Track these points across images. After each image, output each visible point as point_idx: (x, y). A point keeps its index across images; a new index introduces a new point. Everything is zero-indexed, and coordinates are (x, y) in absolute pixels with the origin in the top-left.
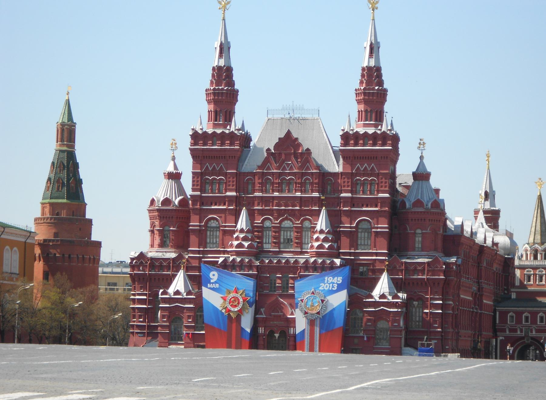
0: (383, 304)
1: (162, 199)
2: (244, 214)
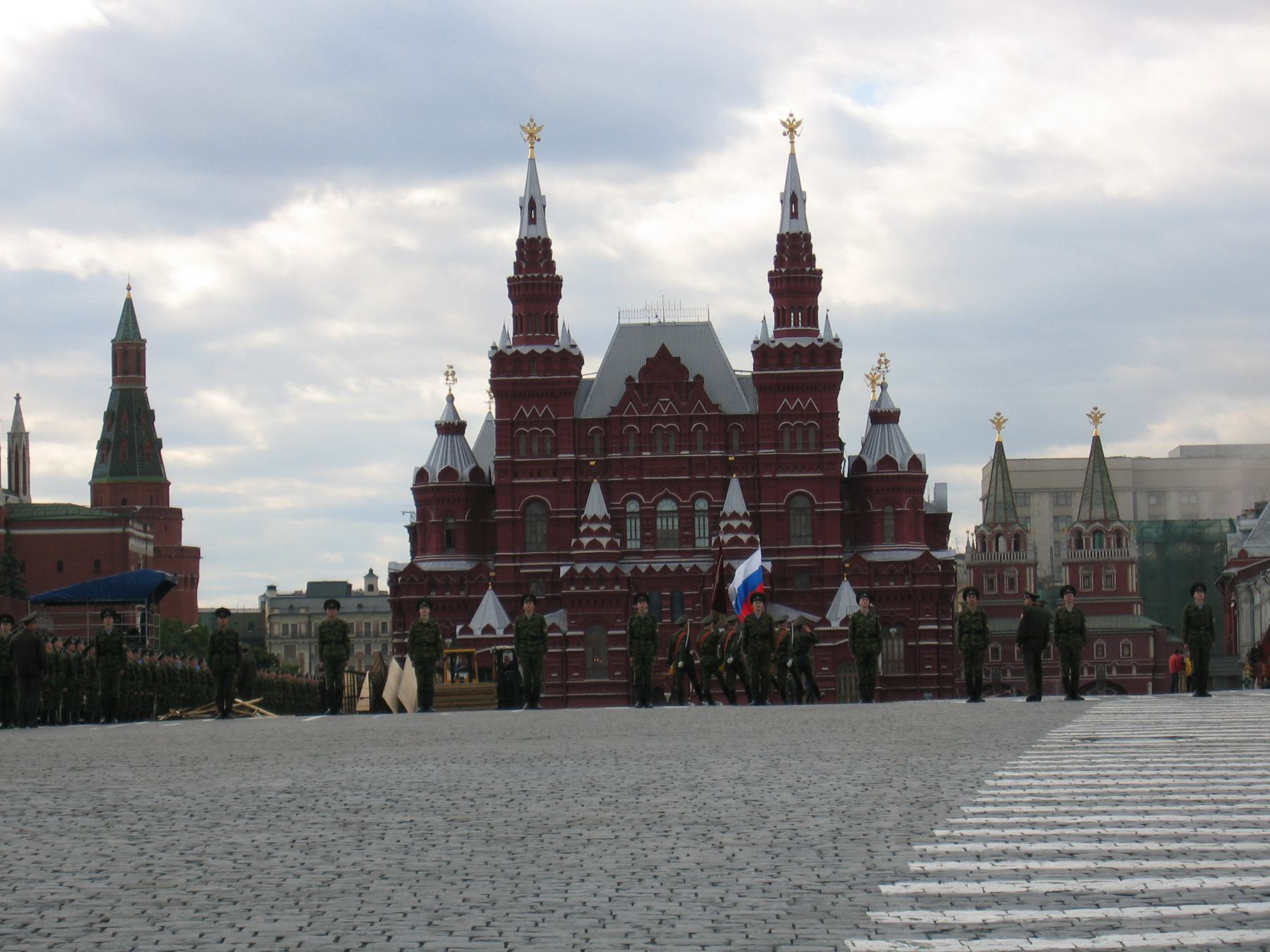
1: (438, 471)
2: (596, 492)
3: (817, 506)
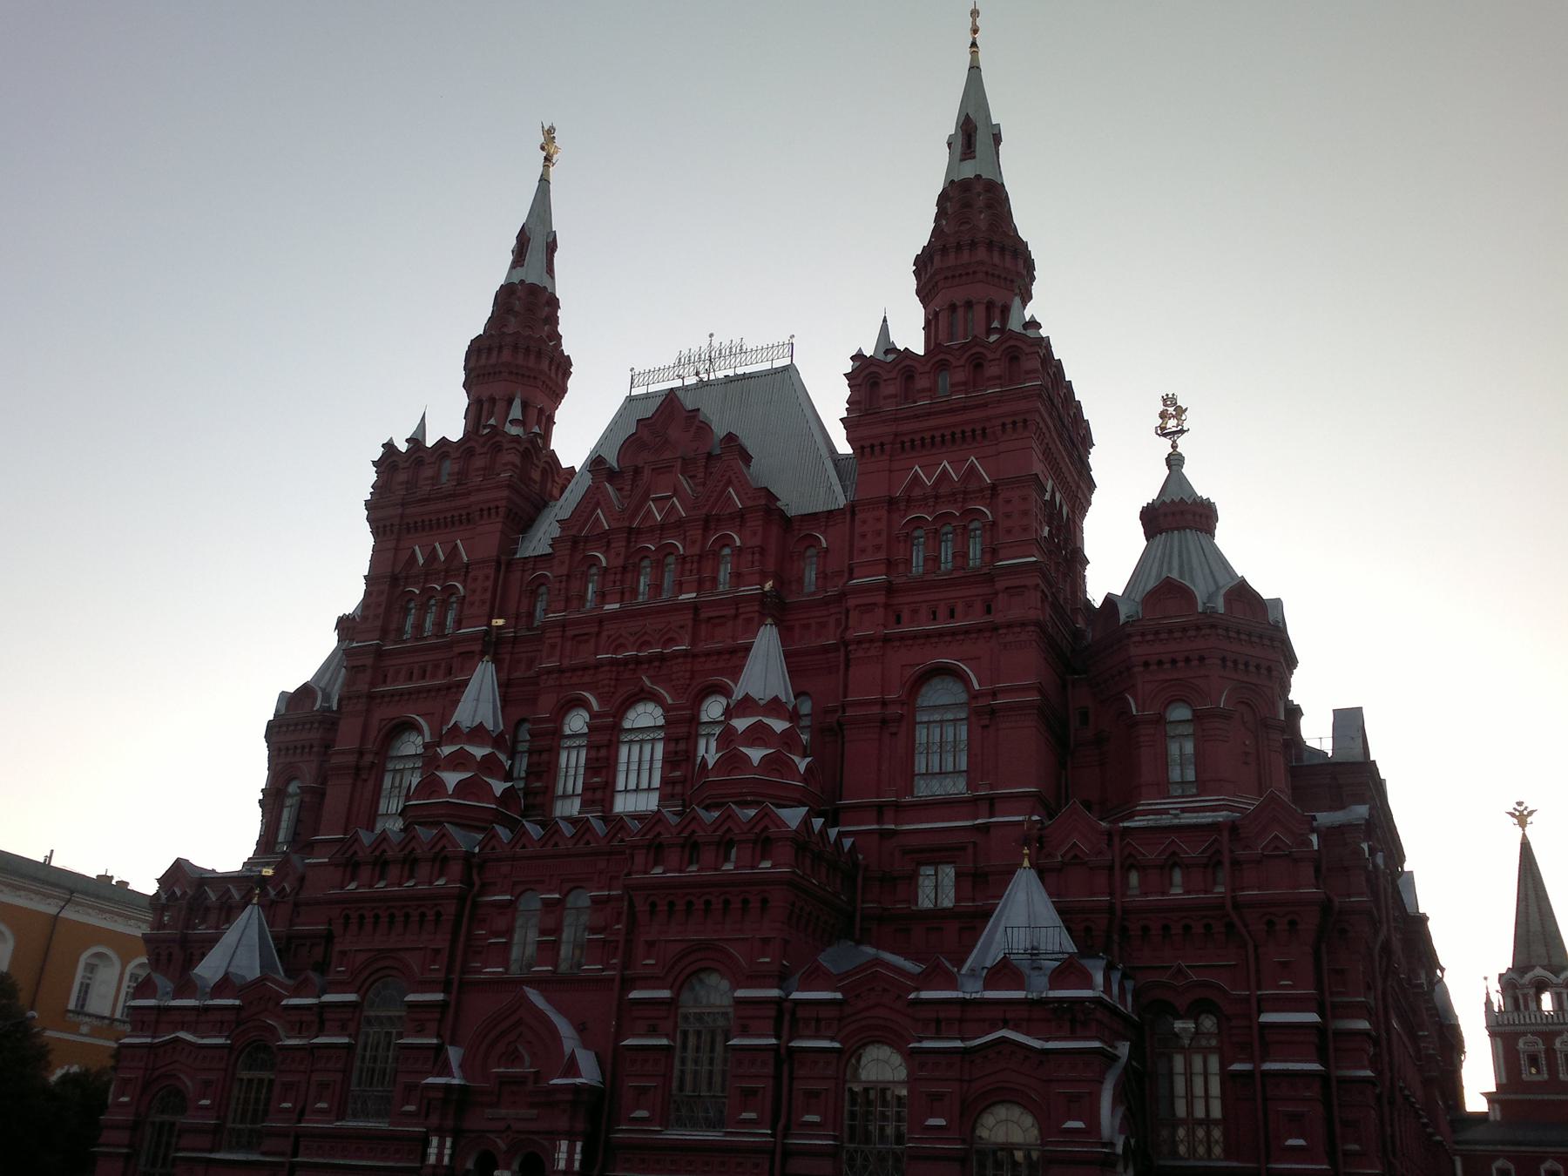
0: (1005, 1013)
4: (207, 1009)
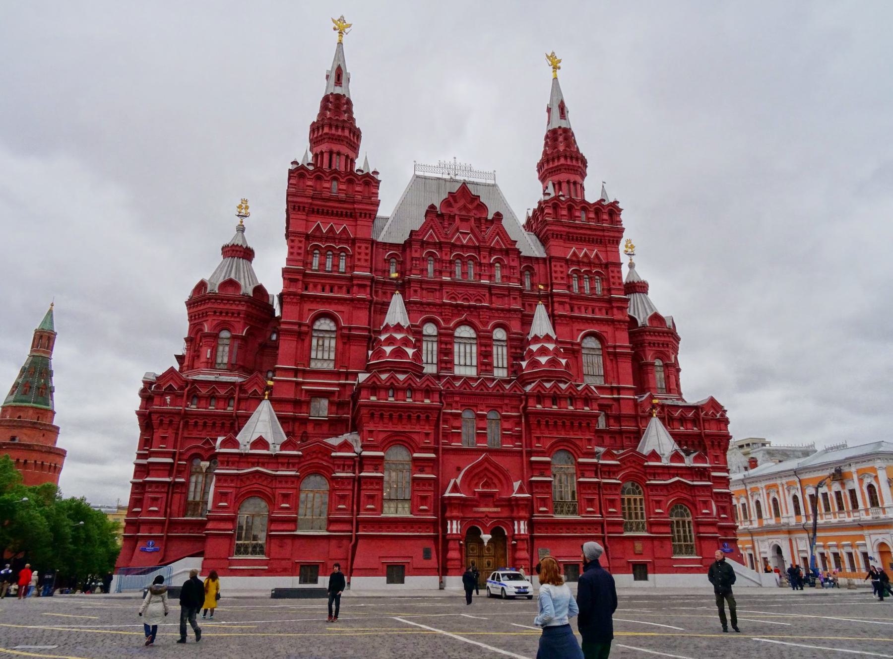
3: (608, 347)
4: (277, 456)
